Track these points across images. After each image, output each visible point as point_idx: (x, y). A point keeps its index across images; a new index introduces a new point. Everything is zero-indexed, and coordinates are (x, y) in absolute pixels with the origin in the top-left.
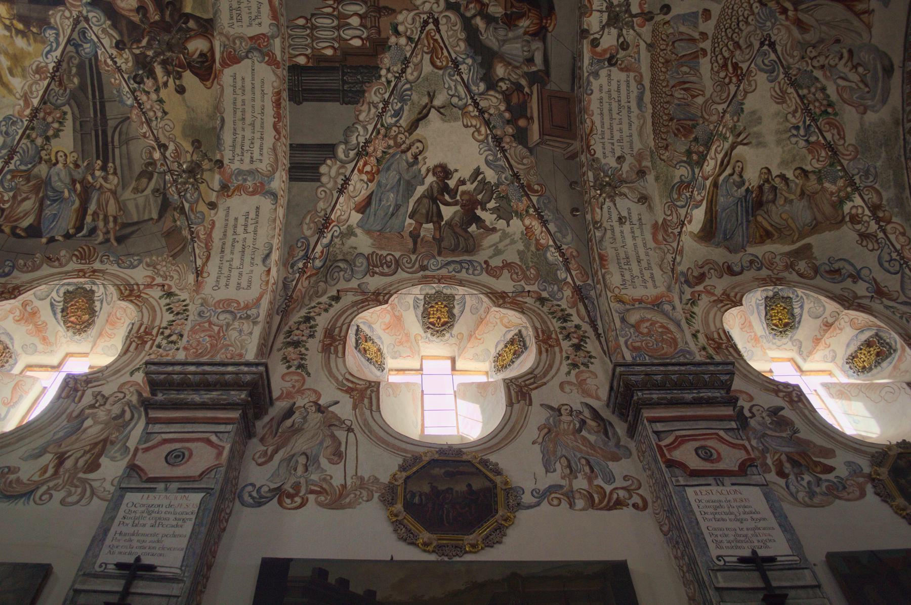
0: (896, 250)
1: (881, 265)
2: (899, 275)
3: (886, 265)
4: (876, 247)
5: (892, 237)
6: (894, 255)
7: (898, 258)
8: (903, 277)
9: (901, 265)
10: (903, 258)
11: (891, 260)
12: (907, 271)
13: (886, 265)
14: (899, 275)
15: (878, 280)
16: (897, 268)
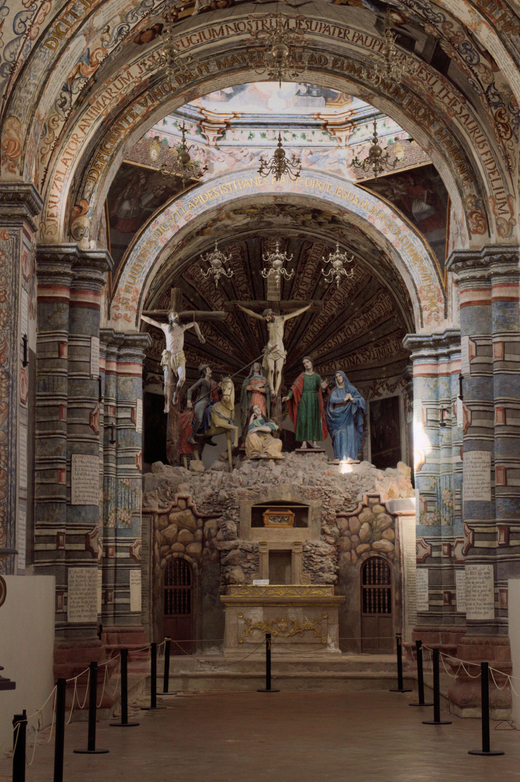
0: (33, 23)
1: (16, 18)
2: (16, 36)
3: (18, 21)
4: (27, 5)
5: (41, 11)
6: (28, 23)
7: (28, 27)
8: (16, 40)
9: (24, 33)
10: (29, 30)
11: (24, 23)
12: (22, 40)
13: (18, 21)
14: (16, 36)
15: (4, 25)
16: (21, 31)
